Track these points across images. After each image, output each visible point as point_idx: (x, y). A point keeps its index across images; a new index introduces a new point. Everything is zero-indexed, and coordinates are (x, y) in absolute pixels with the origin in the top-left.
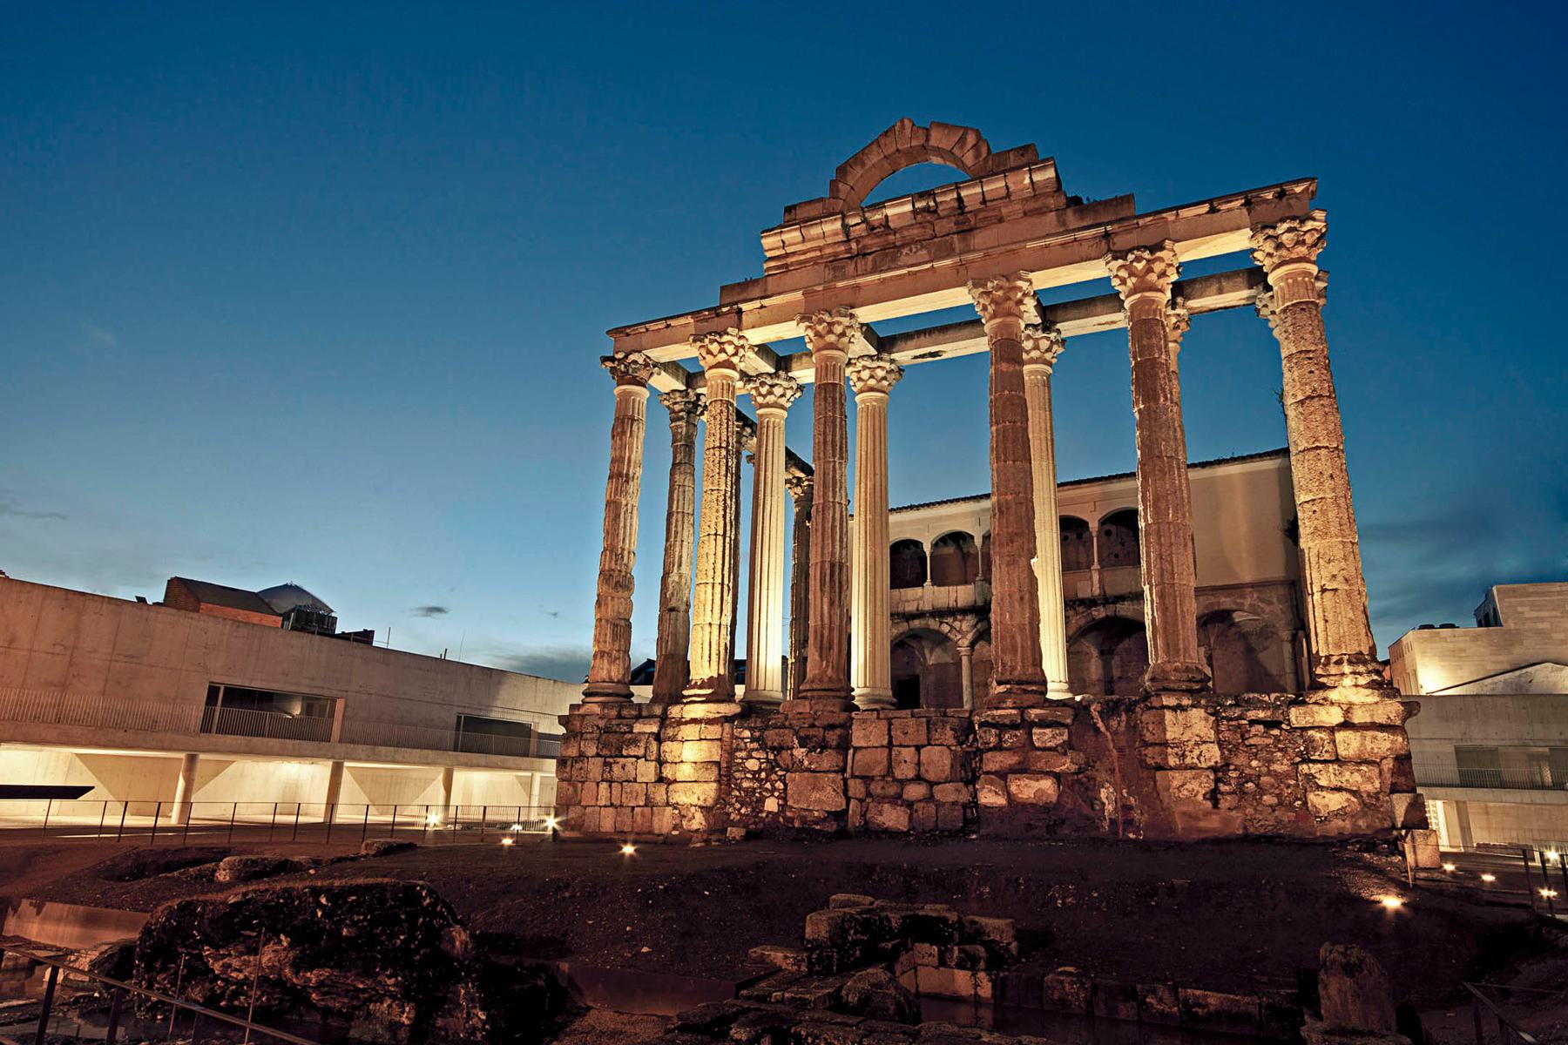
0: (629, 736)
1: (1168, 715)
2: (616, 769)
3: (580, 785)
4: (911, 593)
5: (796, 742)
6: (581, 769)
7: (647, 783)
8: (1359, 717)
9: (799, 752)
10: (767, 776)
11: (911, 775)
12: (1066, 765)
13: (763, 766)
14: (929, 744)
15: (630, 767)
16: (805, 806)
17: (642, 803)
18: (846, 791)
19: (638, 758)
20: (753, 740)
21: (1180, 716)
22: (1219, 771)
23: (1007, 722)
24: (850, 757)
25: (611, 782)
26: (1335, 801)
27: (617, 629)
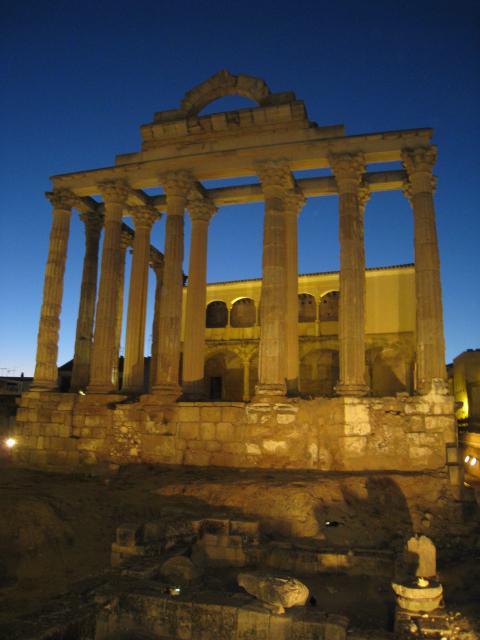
1: (347, 408)
2: (48, 429)
4: (219, 330)
8: (437, 410)
10: (133, 435)
12: (295, 434)
14: (221, 421)
21: (353, 408)
22: (370, 437)
23: (264, 410)
25: (44, 436)
26: (422, 451)
27: (48, 348)
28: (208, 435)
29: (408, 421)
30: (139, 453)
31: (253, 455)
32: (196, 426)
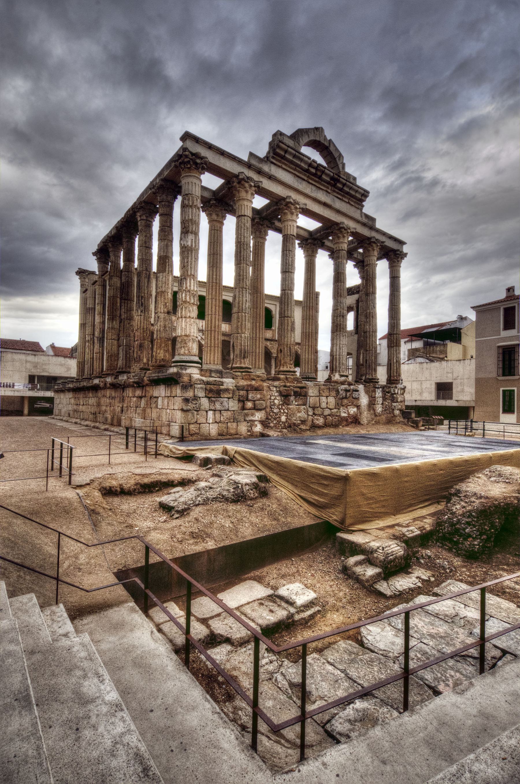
0: (222, 387)
3: (196, 413)
5: (293, 393)
6: (196, 404)
7: (234, 411)
9: (292, 398)
11: (325, 407)
13: (280, 403)
15: (225, 404)
16: (295, 419)
17: (232, 420)
18: (307, 413)
19: (229, 398)
20: (277, 391)
24: (308, 400)
25: (215, 410)
28: (324, 405)
29: (393, 397)
30: (286, 419)
31: (344, 417)
32: (318, 399)
